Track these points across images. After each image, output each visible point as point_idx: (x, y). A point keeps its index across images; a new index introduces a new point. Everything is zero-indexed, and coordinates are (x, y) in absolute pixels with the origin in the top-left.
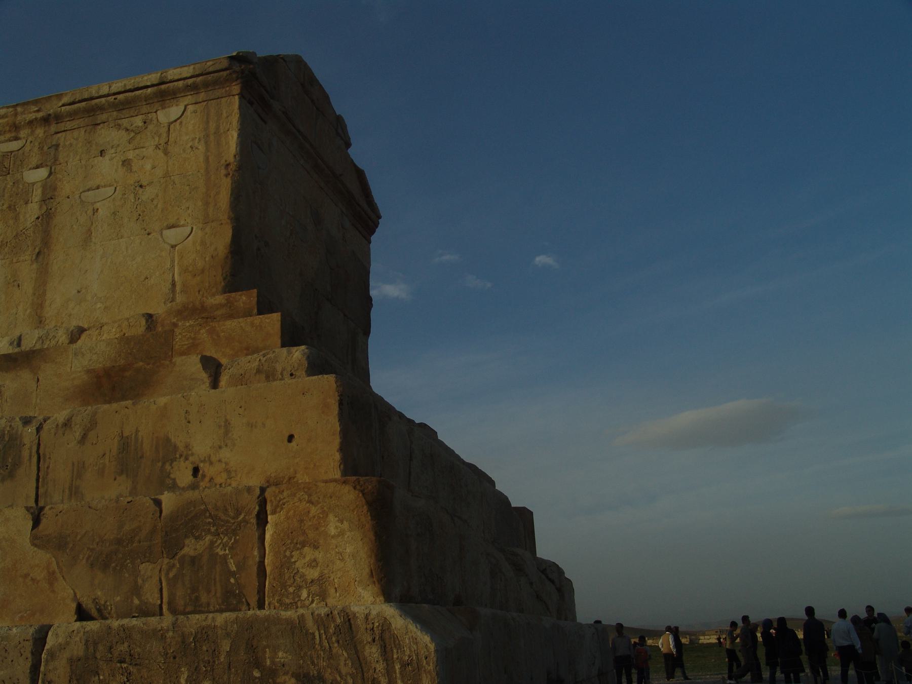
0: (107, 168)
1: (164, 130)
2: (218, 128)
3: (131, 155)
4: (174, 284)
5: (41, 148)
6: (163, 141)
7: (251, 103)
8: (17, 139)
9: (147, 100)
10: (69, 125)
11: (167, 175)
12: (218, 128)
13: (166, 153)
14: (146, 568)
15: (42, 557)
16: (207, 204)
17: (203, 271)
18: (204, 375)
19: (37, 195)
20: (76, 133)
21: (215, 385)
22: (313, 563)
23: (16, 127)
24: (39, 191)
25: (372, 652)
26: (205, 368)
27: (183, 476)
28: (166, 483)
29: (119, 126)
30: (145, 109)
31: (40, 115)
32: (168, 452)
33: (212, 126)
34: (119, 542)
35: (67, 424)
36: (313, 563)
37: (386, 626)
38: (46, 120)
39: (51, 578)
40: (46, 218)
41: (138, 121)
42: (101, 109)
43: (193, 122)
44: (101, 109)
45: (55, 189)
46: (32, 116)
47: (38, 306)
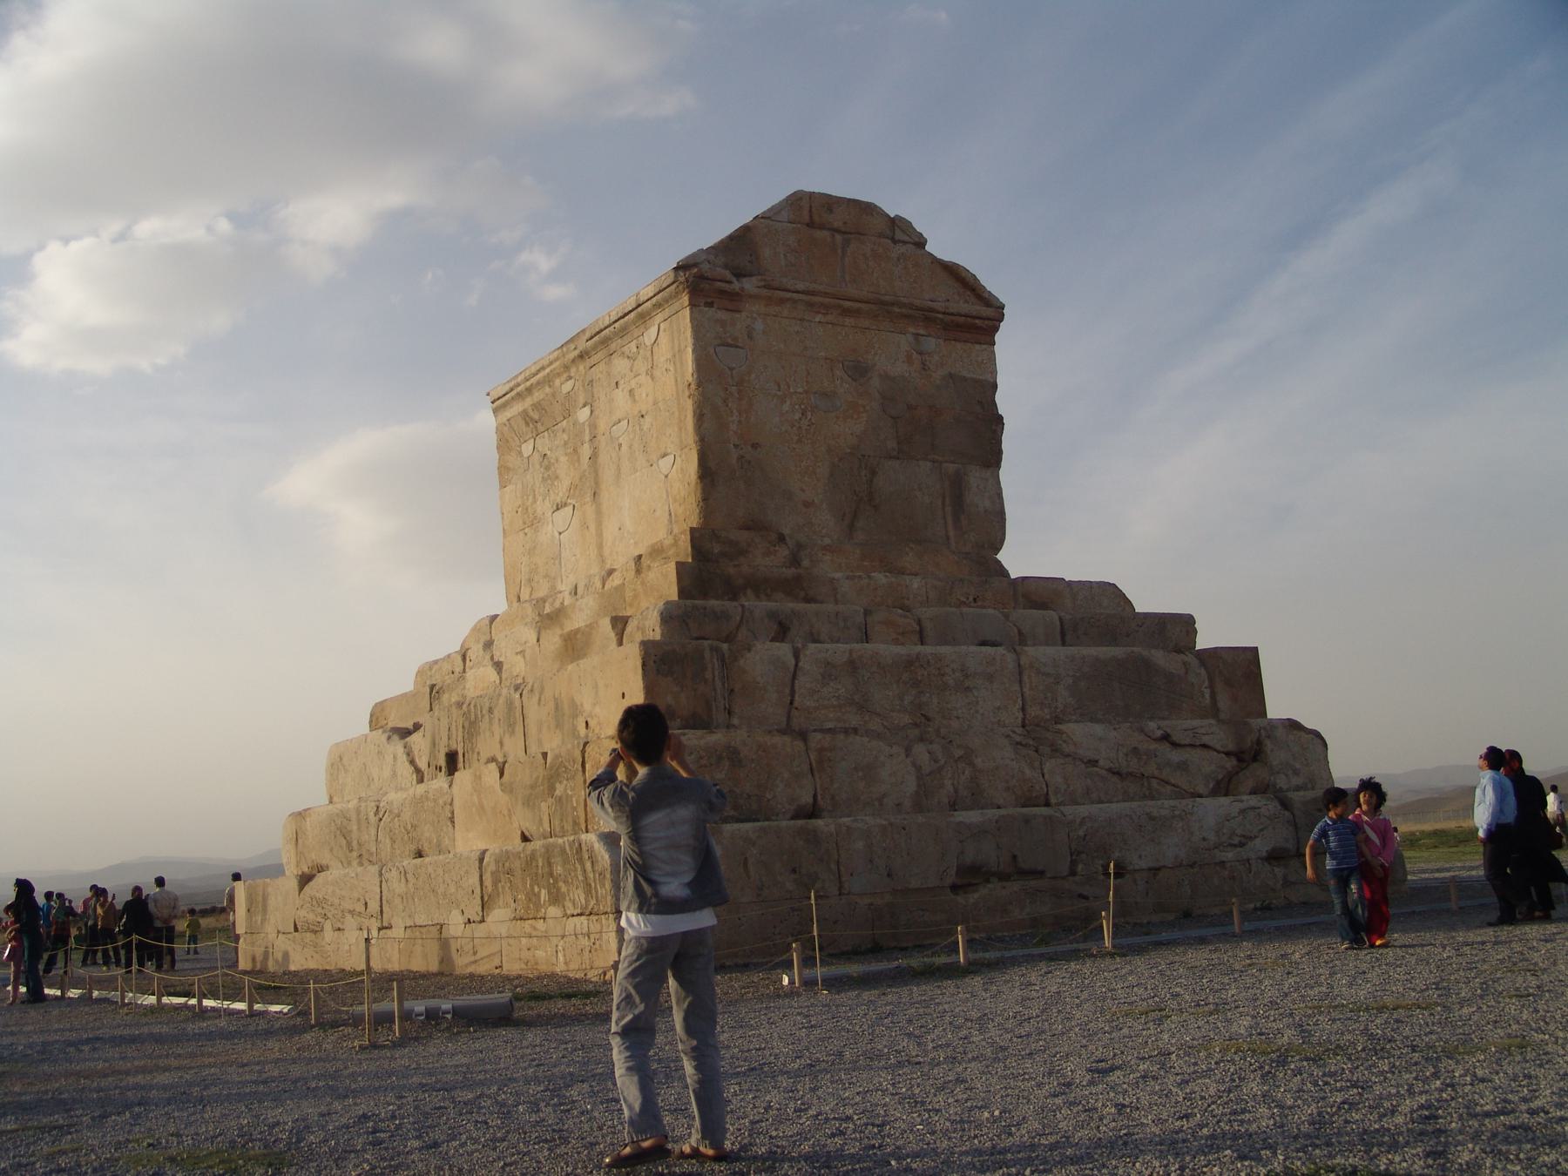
0: (620, 396)
3: (633, 384)
7: (710, 305)
8: (570, 378)
14: (543, 804)
15: (503, 799)
18: (613, 635)
21: (620, 643)
25: (588, 865)
26: (613, 627)
31: (576, 353)
32: (576, 710)
38: (581, 356)
40: (594, 457)
41: (633, 345)
43: (664, 340)
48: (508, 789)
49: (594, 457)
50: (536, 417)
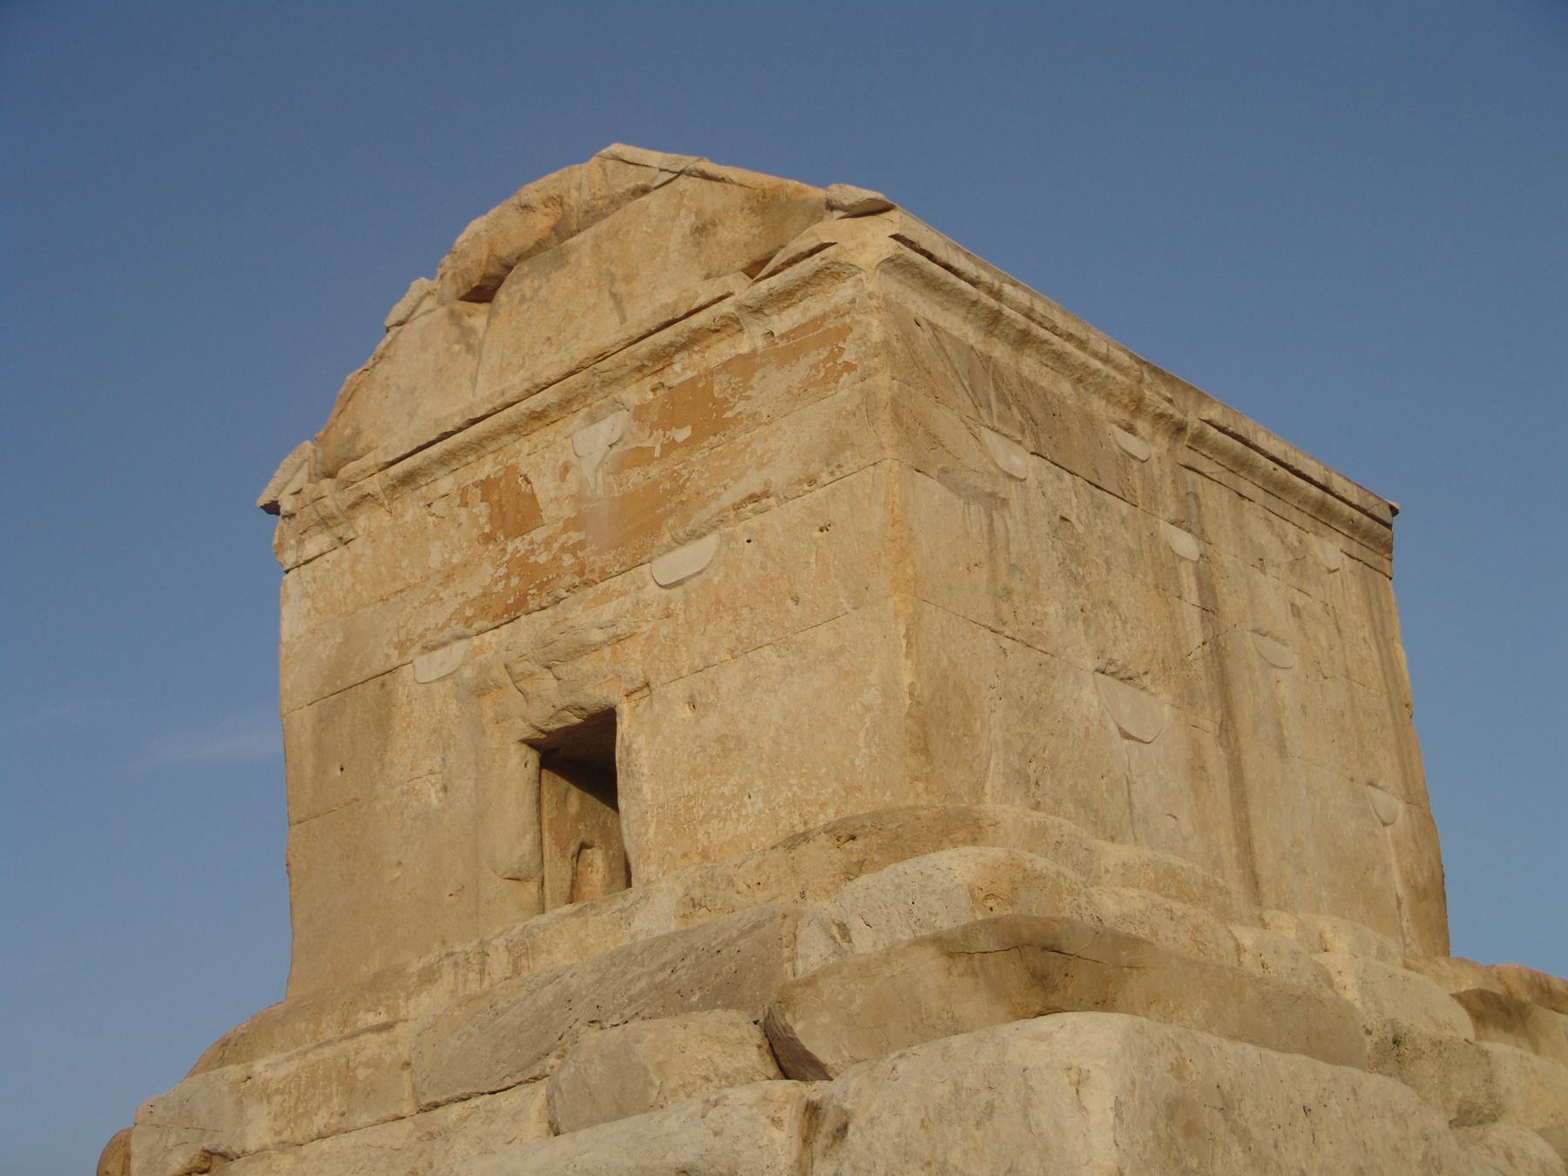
3: (1300, 600)
8: (1130, 429)
16: (1403, 765)
19: (1189, 583)
20: (1215, 488)
30: (1296, 517)
40: (1217, 650)
41: (1292, 533)
43: (1355, 590)
47: (1246, 846)
49: (1217, 650)
50: (1040, 416)
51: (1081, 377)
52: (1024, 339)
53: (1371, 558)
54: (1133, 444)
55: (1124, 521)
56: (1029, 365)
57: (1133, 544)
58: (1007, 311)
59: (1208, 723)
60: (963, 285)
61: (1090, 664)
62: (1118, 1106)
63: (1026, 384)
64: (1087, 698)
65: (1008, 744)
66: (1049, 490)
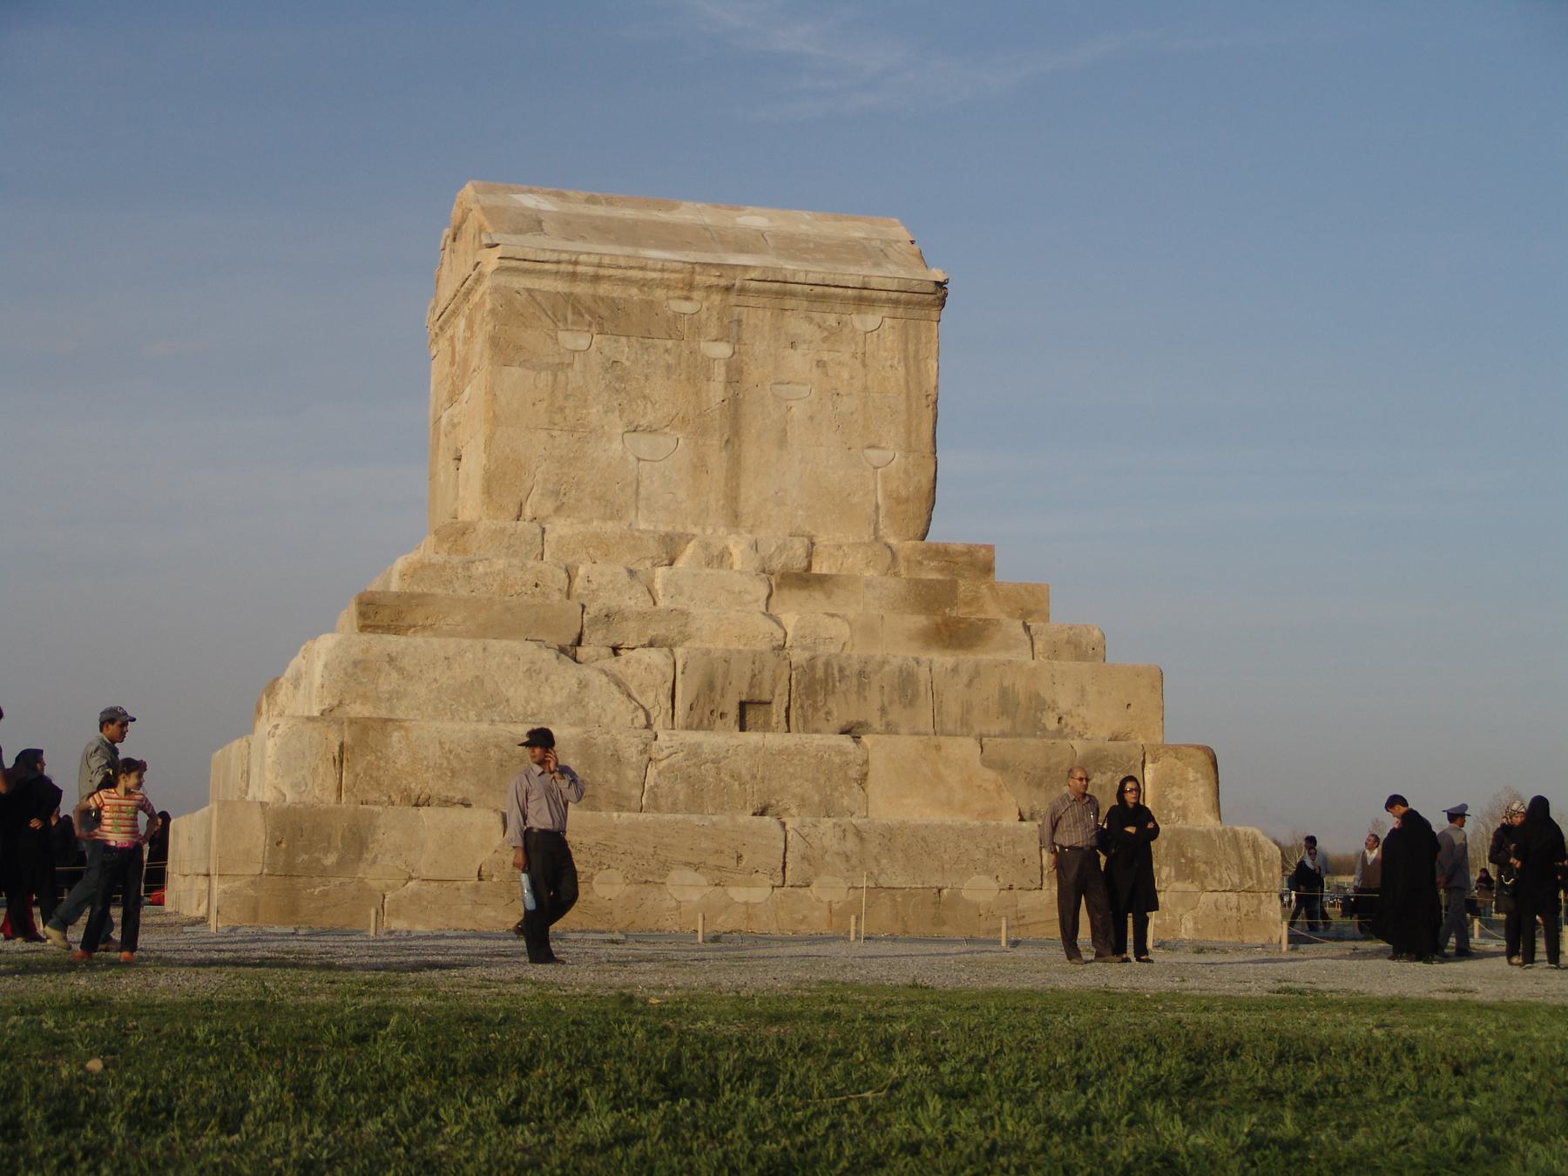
0: (799, 362)
1: (860, 338)
2: (917, 352)
3: (826, 357)
4: (877, 507)
5: (720, 319)
6: (860, 351)
8: (687, 298)
9: (844, 300)
10: (752, 301)
11: (865, 389)
12: (917, 352)
13: (864, 365)
15: (990, 774)
16: (909, 432)
17: (907, 500)
19: (720, 373)
20: (760, 312)
22: (1179, 797)
23: (691, 286)
24: (723, 369)
25: (1248, 853)
27: (1052, 725)
28: (1037, 727)
29: (810, 320)
30: (838, 308)
31: (723, 282)
33: (911, 348)
34: (1048, 769)
35: (955, 670)
36: (1179, 797)
37: (1255, 840)
38: (728, 289)
39: (999, 790)
40: (734, 406)
41: (831, 320)
42: (793, 295)
43: (890, 338)
44: (793, 295)
45: (741, 372)
46: (714, 281)
48: (1002, 766)
50: (604, 312)
51: (643, 284)
52: (596, 278)
53: (917, 313)
54: (687, 307)
55: (667, 351)
56: (603, 289)
57: (670, 359)
58: (580, 269)
59: (715, 442)
60: (547, 266)
61: (620, 431)
62: (326, 666)
63: (596, 299)
64: (614, 447)
65: (546, 481)
66: (606, 351)
